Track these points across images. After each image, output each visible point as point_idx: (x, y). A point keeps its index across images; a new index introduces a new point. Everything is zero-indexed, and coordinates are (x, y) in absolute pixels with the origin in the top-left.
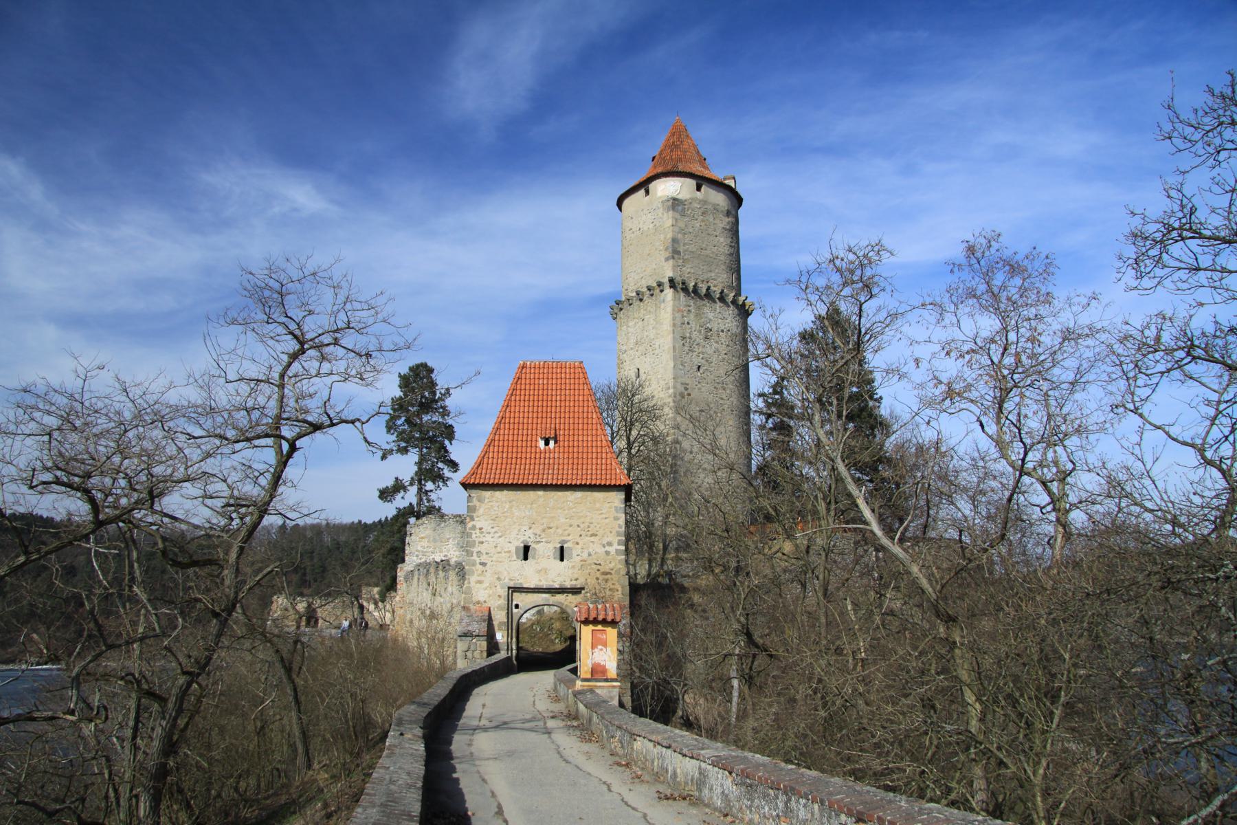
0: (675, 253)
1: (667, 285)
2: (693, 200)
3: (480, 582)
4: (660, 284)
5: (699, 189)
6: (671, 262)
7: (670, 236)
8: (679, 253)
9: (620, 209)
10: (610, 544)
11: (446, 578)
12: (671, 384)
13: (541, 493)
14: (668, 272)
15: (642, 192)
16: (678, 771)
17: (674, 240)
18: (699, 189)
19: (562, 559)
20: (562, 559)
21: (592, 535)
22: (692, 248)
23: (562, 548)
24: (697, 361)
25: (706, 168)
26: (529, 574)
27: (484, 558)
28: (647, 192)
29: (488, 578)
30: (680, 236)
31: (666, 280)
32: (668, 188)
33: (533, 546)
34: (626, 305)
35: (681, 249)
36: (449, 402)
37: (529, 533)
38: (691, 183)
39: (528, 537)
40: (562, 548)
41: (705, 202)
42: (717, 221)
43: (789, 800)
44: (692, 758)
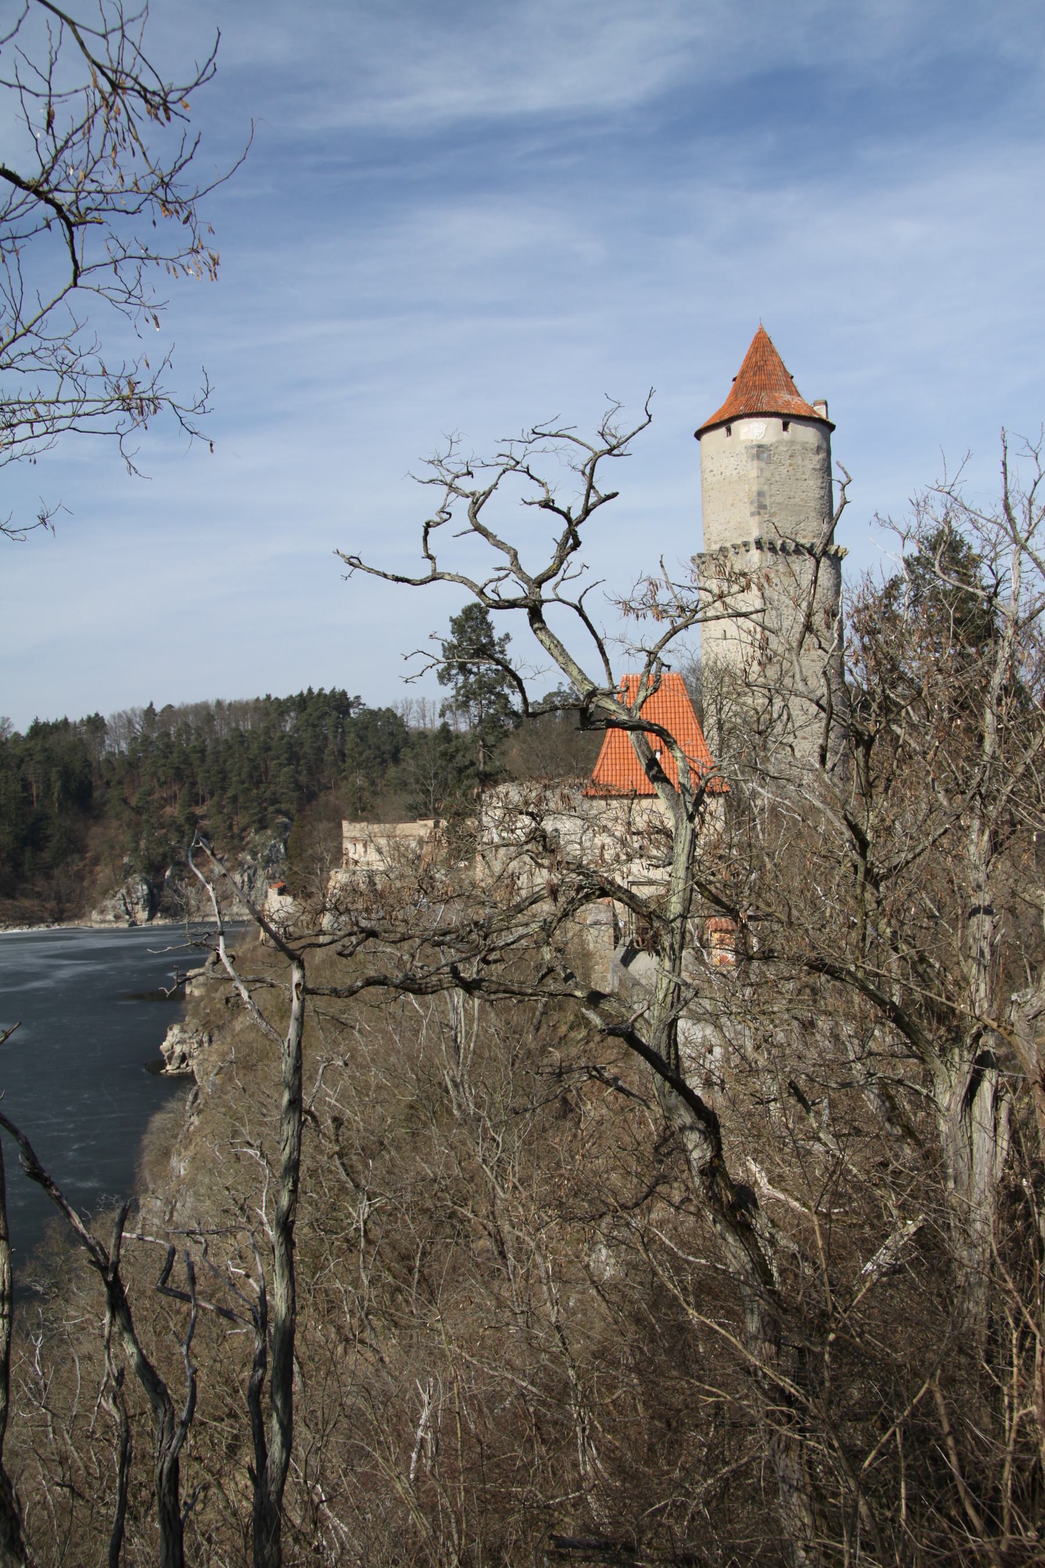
1: (753, 546)
5: (785, 427)
6: (757, 517)
7: (755, 488)
8: (764, 507)
14: (755, 534)
15: (723, 430)
17: (760, 494)
18: (785, 427)
22: (779, 499)
28: (729, 430)
30: (766, 488)
32: (754, 430)
35: (767, 502)
38: (778, 422)
41: (792, 443)
42: (807, 462)
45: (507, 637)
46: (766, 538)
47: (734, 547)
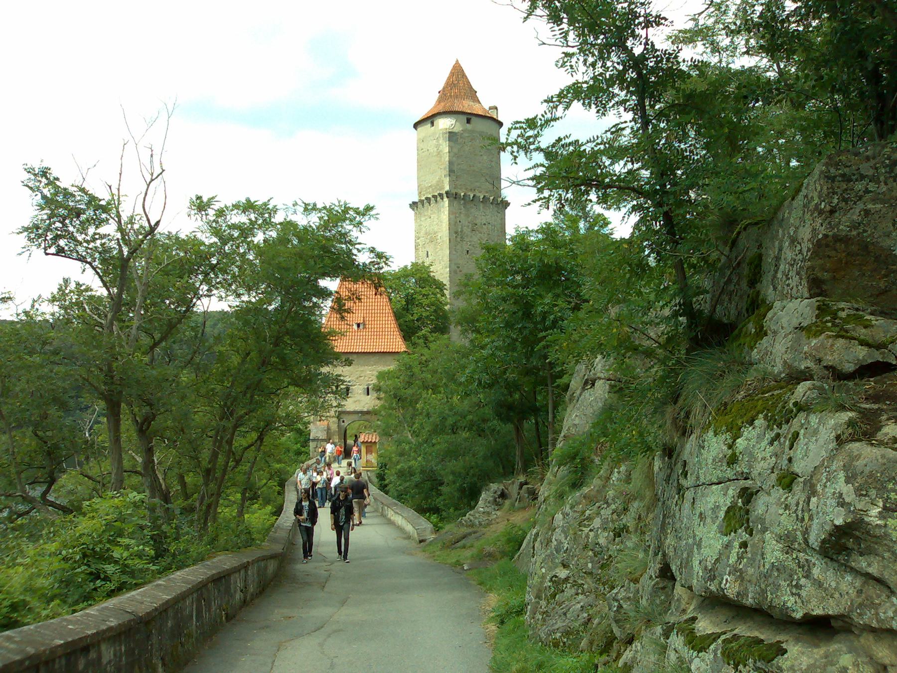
0: (451, 171)
1: (445, 195)
7: (447, 159)
12: (448, 265)
18: (468, 121)
19: (368, 394)
24: (466, 248)
34: (420, 205)
38: (464, 118)
46: (454, 191)
47: (433, 196)
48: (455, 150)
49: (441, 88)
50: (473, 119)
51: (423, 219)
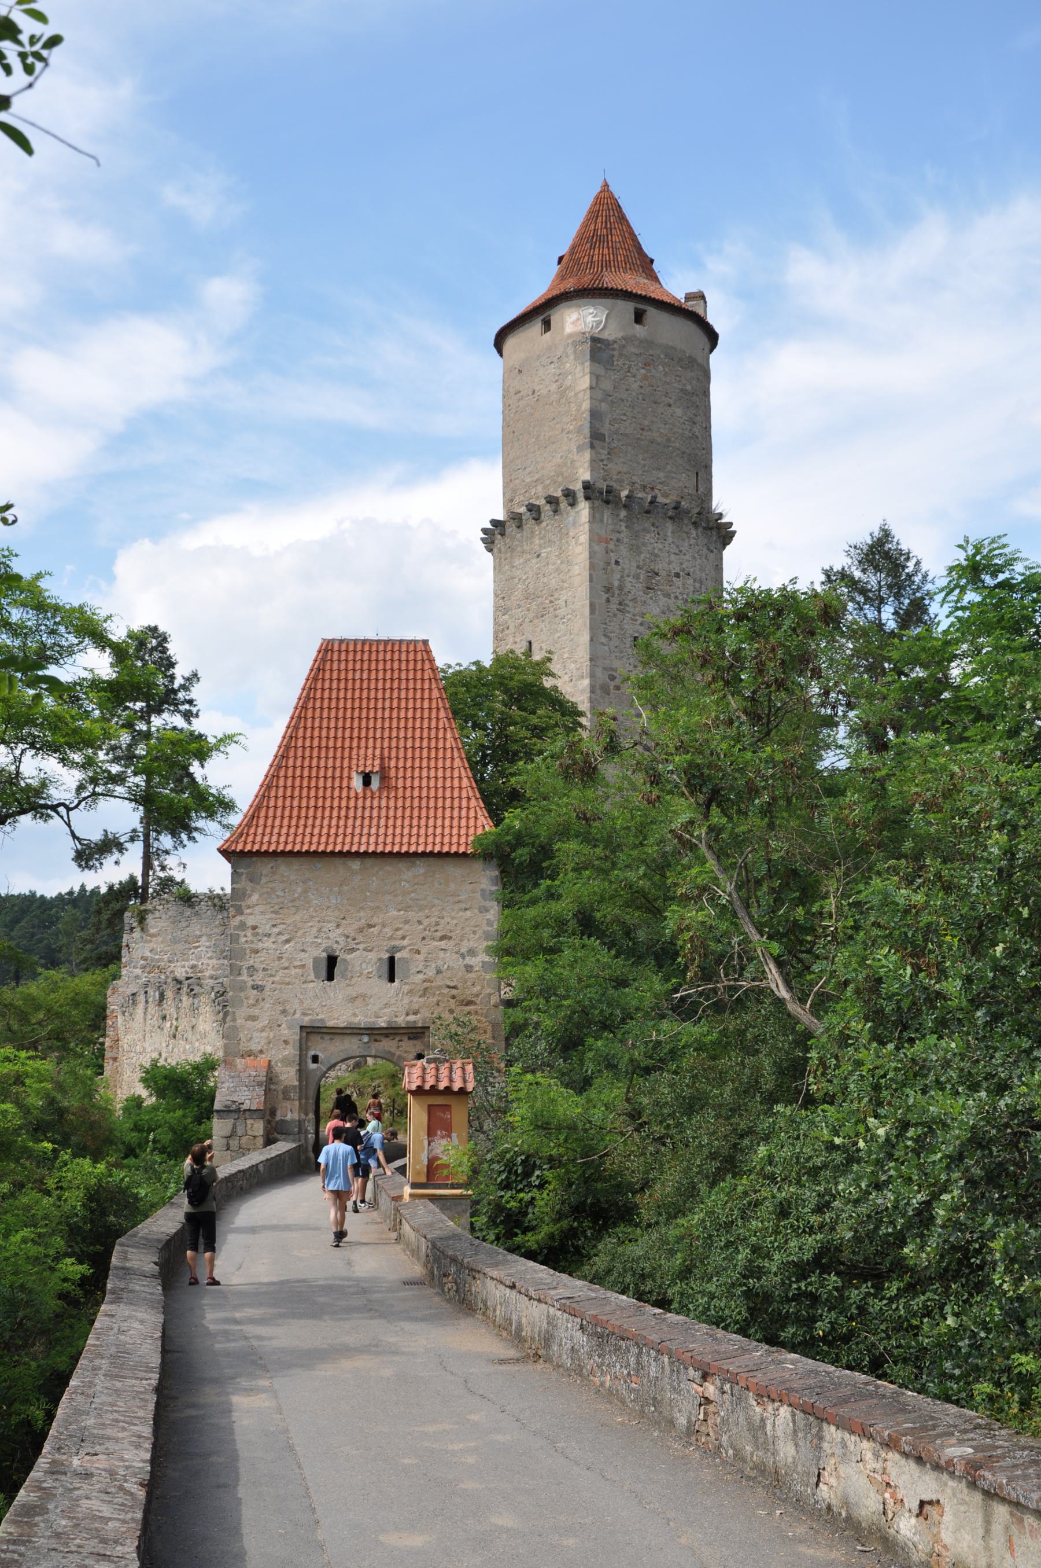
0: (596, 437)
1: (580, 495)
2: (628, 339)
3: (253, 1018)
4: (569, 494)
7: (586, 405)
9: (500, 352)
10: (472, 952)
11: (194, 1009)
12: (586, 668)
13: (356, 865)
15: (537, 326)
16: (524, 1320)
17: (595, 415)
18: (639, 317)
19: (392, 979)
20: (392, 979)
21: (443, 938)
23: (392, 960)
25: (656, 279)
26: (336, 1005)
27: (259, 978)
28: (547, 325)
29: (266, 1012)
30: (604, 406)
31: (578, 487)
33: (342, 956)
34: (511, 529)
35: (606, 429)
36: (196, 692)
37: (335, 934)
38: (627, 308)
39: (334, 939)
40: (392, 960)
41: (648, 343)
43: (640, 1353)
44: (539, 1301)
45: (194, 677)
48: (607, 385)
49: (564, 249)
50: (652, 312)
51: (517, 562)
